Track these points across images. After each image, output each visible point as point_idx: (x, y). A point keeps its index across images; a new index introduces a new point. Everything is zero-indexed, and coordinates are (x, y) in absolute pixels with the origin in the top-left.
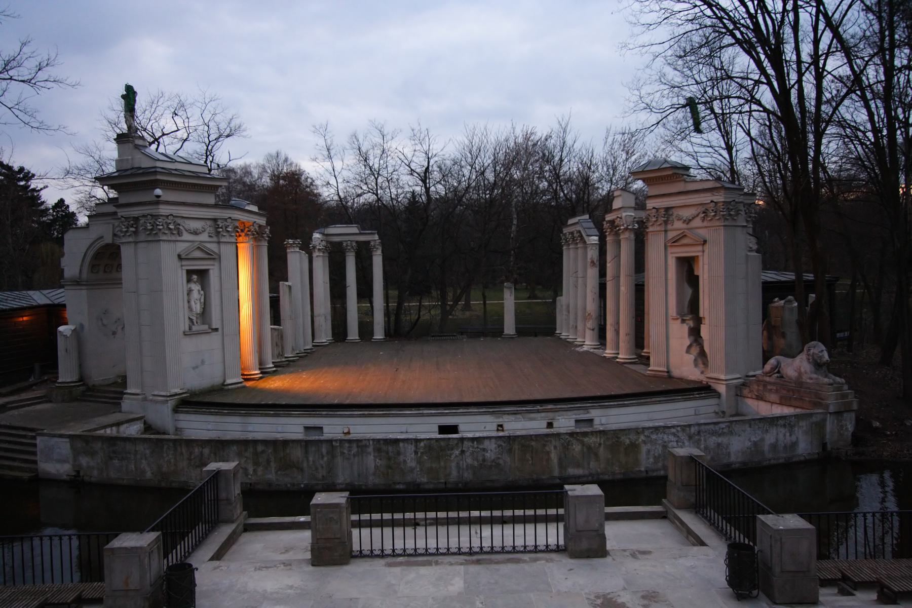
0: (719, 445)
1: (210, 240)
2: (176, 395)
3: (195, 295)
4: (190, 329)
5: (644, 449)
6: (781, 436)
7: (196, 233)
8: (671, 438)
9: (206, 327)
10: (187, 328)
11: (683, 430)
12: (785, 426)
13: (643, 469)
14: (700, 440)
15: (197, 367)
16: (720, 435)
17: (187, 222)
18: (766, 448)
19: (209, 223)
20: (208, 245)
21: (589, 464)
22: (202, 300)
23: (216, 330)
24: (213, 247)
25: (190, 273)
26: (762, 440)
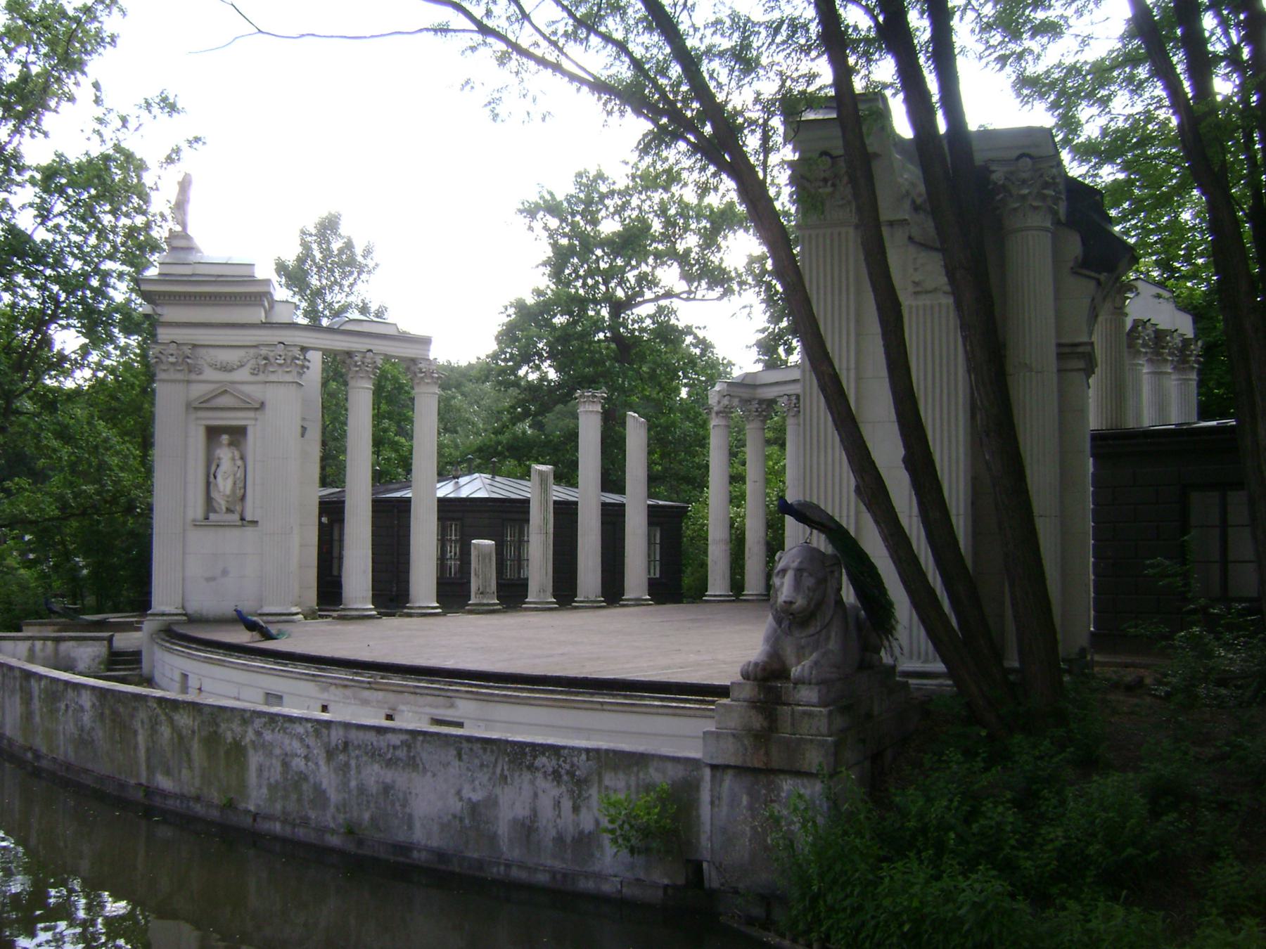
0: (387, 789)
2: (163, 615)
5: (254, 759)
6: (545, 803)
7: (226, 368)
8: (296, 745)
10: (200, 514)
11: (317, 733)
12: (556, 776)
13: (252, 808)
14: (347, 765)
15: (213, 579)
16: (390, 763)
17: (212, 352)
18: (503, 829)
19: (252, 351)
20: (246, 388)
21: (180, 772)
22: (240, 474)
23: (255, 523)
24: (256, 392)
25: (213, 433)
26: (492, 802)
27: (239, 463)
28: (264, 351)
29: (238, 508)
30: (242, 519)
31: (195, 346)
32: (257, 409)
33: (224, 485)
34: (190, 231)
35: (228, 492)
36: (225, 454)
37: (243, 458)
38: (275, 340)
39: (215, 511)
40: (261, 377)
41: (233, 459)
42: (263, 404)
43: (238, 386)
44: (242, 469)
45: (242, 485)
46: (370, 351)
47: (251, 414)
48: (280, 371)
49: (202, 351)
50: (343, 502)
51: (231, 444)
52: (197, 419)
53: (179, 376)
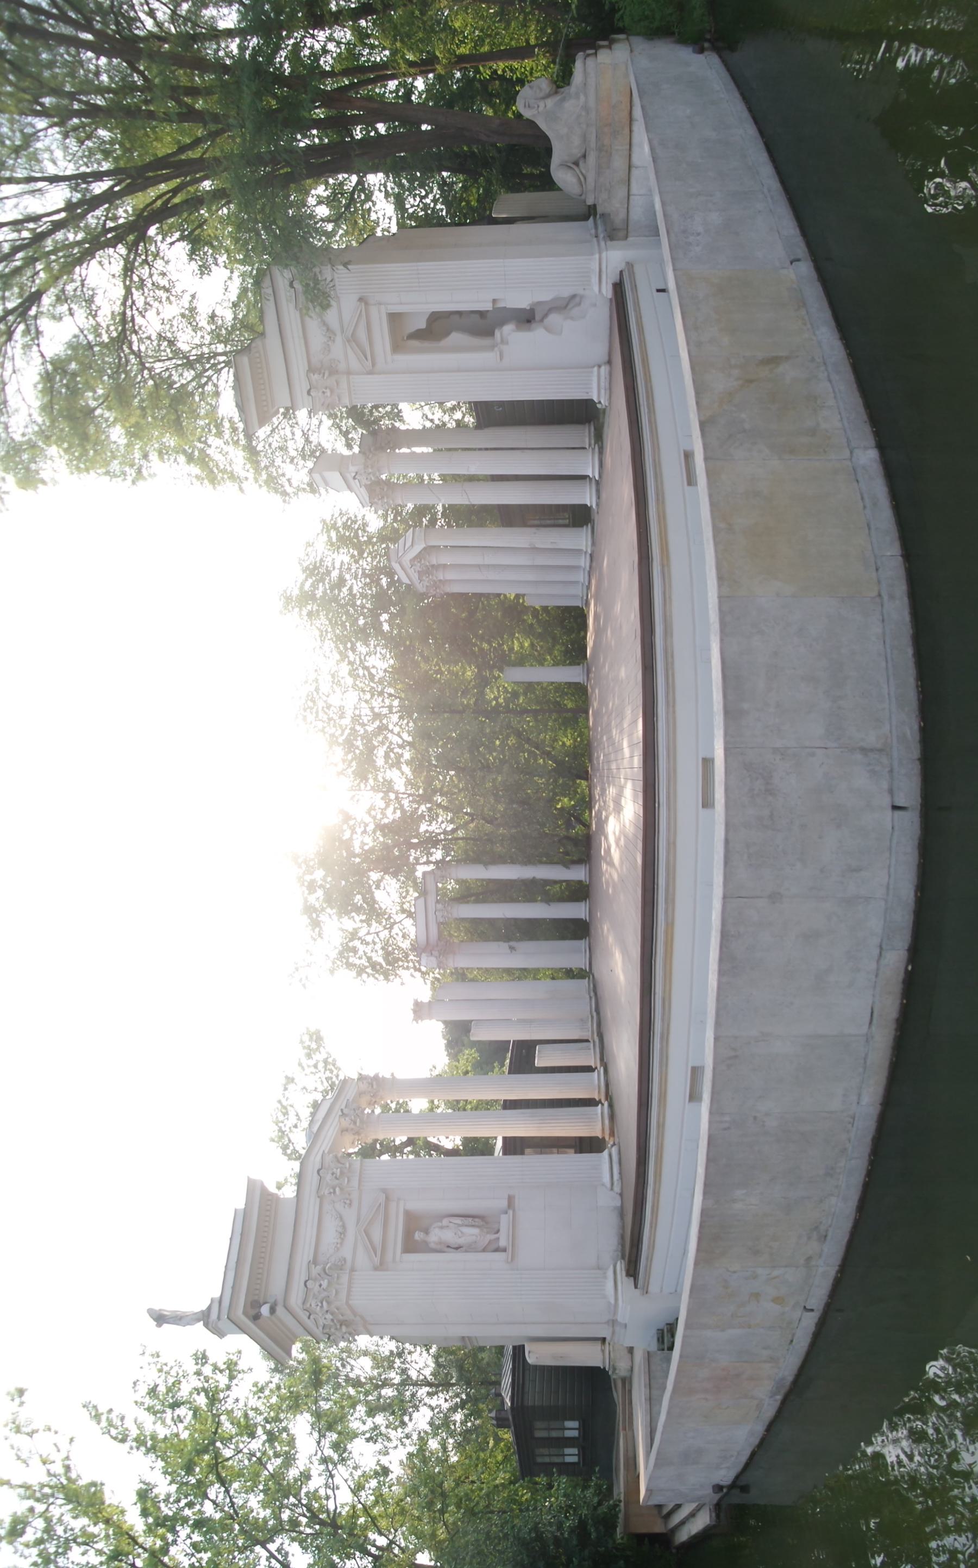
1: (355, 1204)
3: (448, 1236)
4: (504, 1250)
7: (342, 1233)
9: (505, 1221)
22: (458, 1221)
23: (511, 1199)
25: (410, 1246)
27: (445, 1222)
32: (387, 1198)
35: (475, 1231)
36: (436, 1235)
38: (316, 1178)
41: (442, 1228)
42: (384, 1191)
45: (470, 1219)
51: (427, 1232)
53: (345, 1279)
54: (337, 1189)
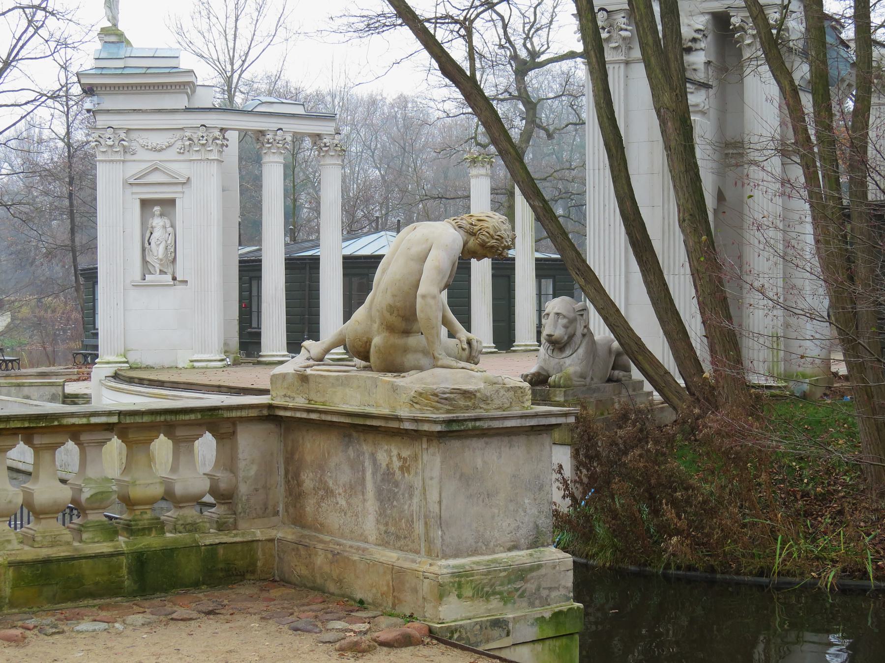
1: (182, 157)
7: (155, 150)
10: (138, 276)
17: (144, 135)
19: (179, 134)
22: (170, 240)
23: (185, 282)
24: (182, 169)
25: (146, 204)
27: (170, 230)
28: (188, 134)
29: (170, 270)
30: (174, 279)
31: (129, 130)
33: (158, 251)
34: (121, 27)
36: (157, 222)
37: (173, 226)
38: (198, 123)
39: (151, 273)
40: (186, 156)
41: (164, 227)
43: (168, 165)
44: (171, 238)
45: (172, 250)
46: (281, 129)
47: (179, 189)
48: (203, 150)
49: (134, 135)
50: (260, 261)
51: (162, 215)
52: (133, 193)
54: (188, 143)
